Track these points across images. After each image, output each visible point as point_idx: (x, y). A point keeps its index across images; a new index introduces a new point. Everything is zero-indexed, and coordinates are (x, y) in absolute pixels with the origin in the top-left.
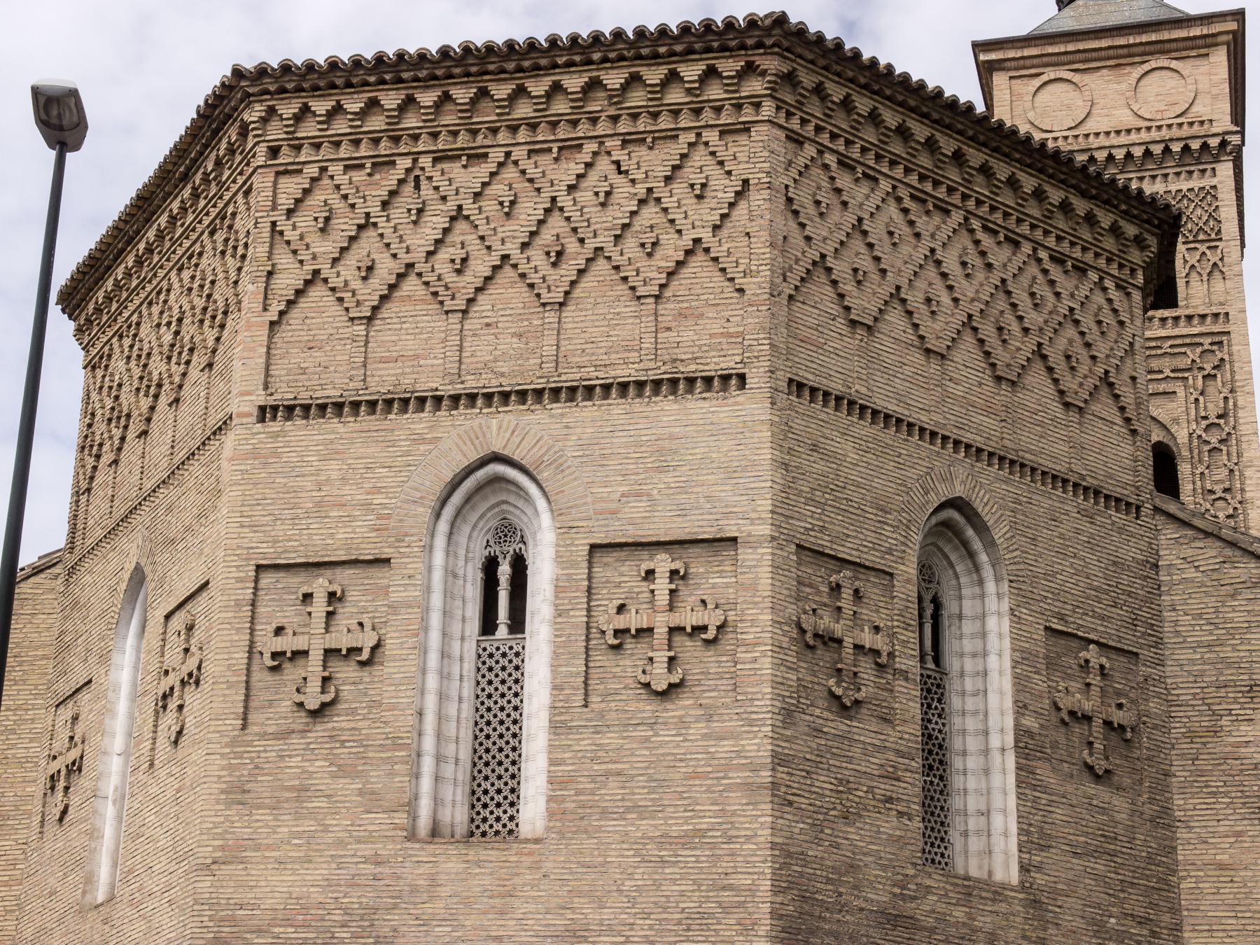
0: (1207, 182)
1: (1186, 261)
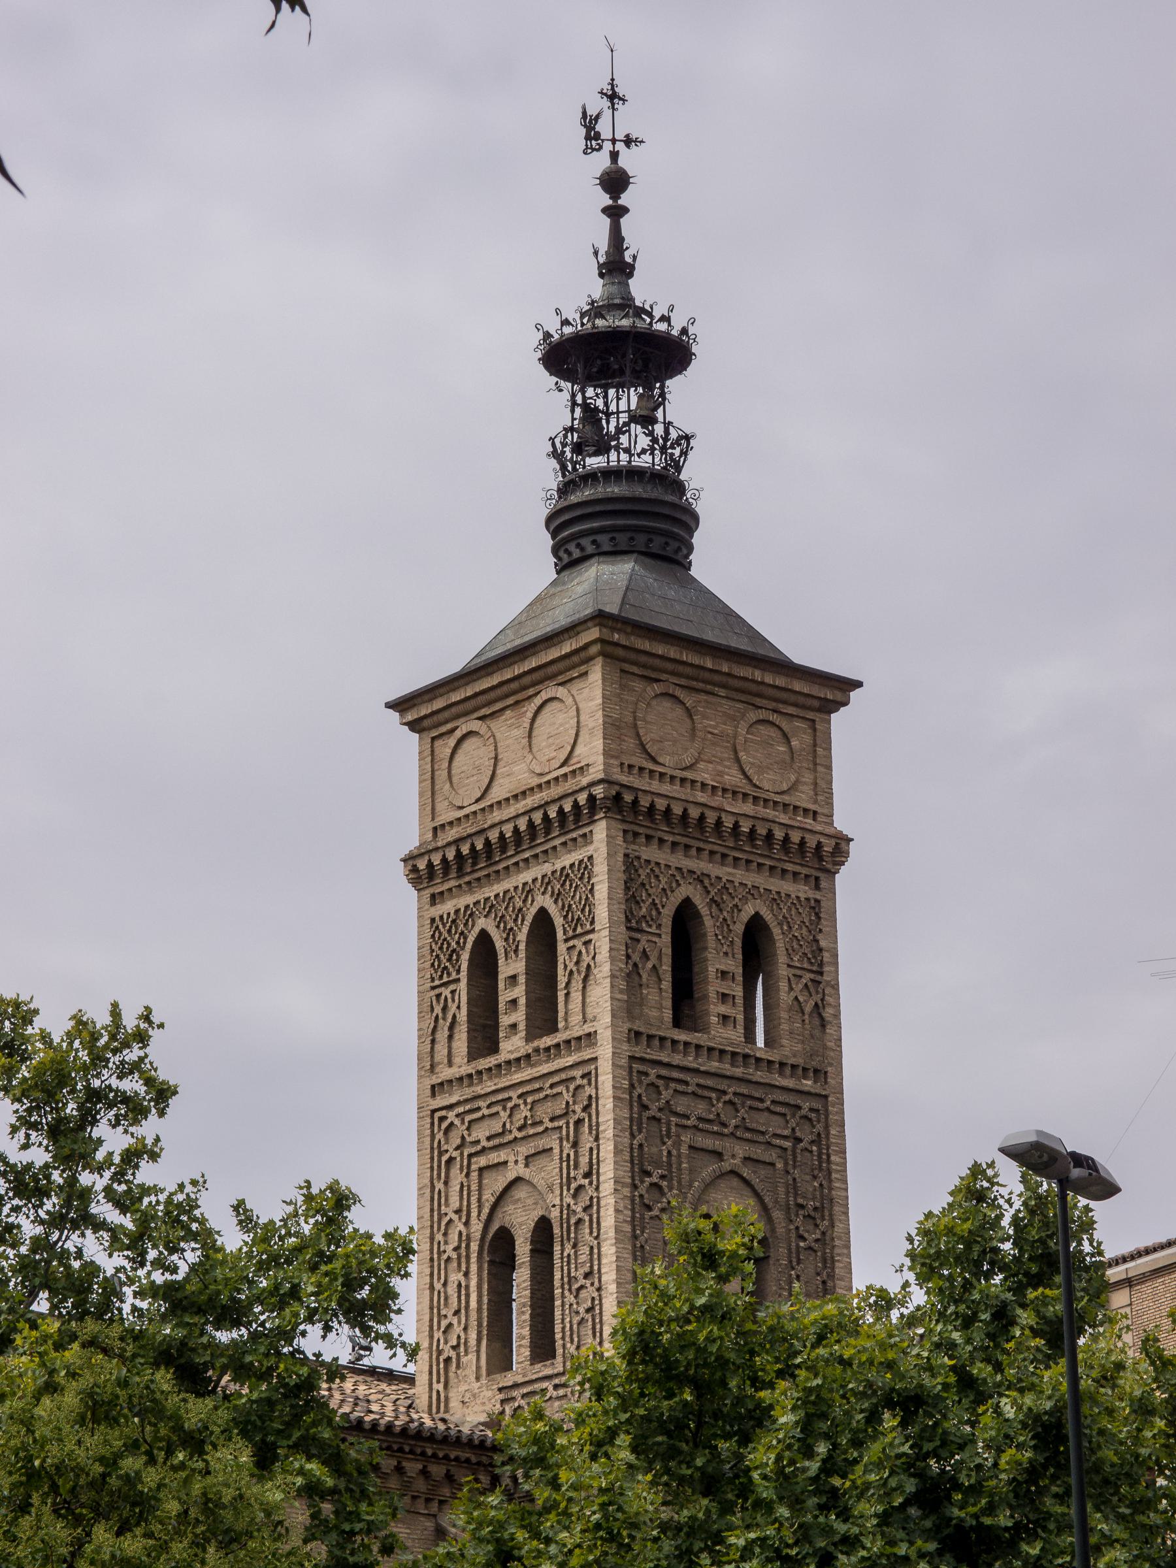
1: (566, 967)
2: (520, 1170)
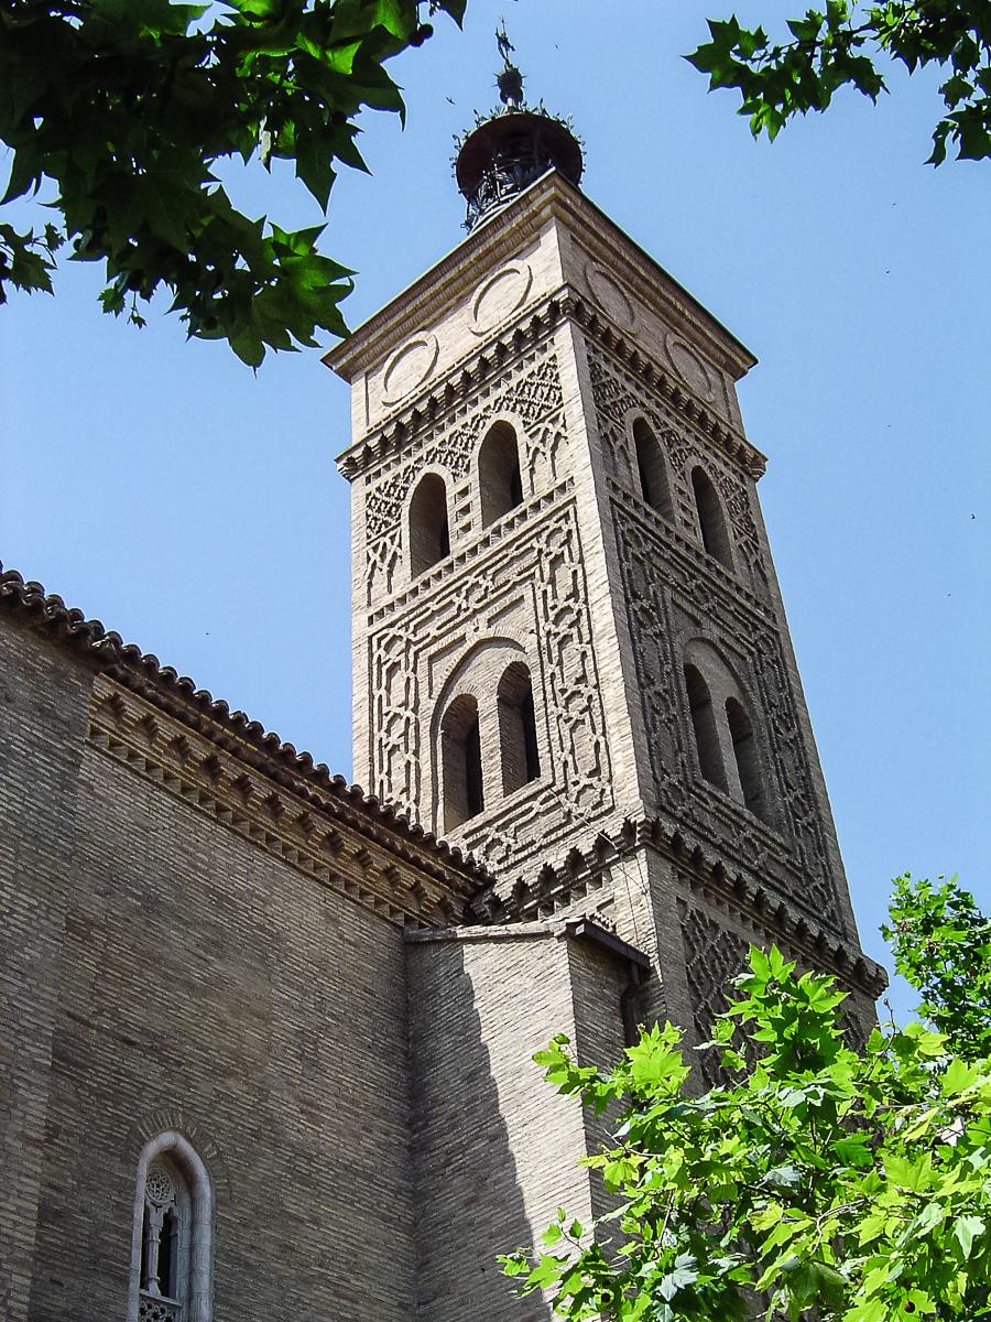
0: (543, 358)
2: (485, 633)
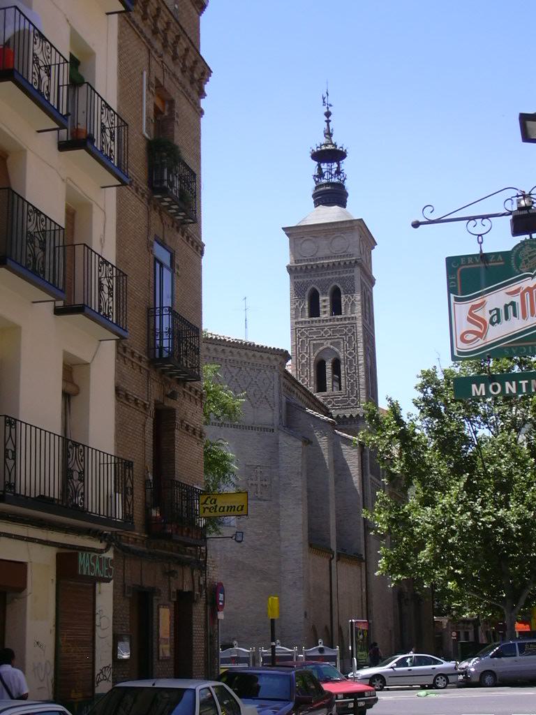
2: (329, 345)
